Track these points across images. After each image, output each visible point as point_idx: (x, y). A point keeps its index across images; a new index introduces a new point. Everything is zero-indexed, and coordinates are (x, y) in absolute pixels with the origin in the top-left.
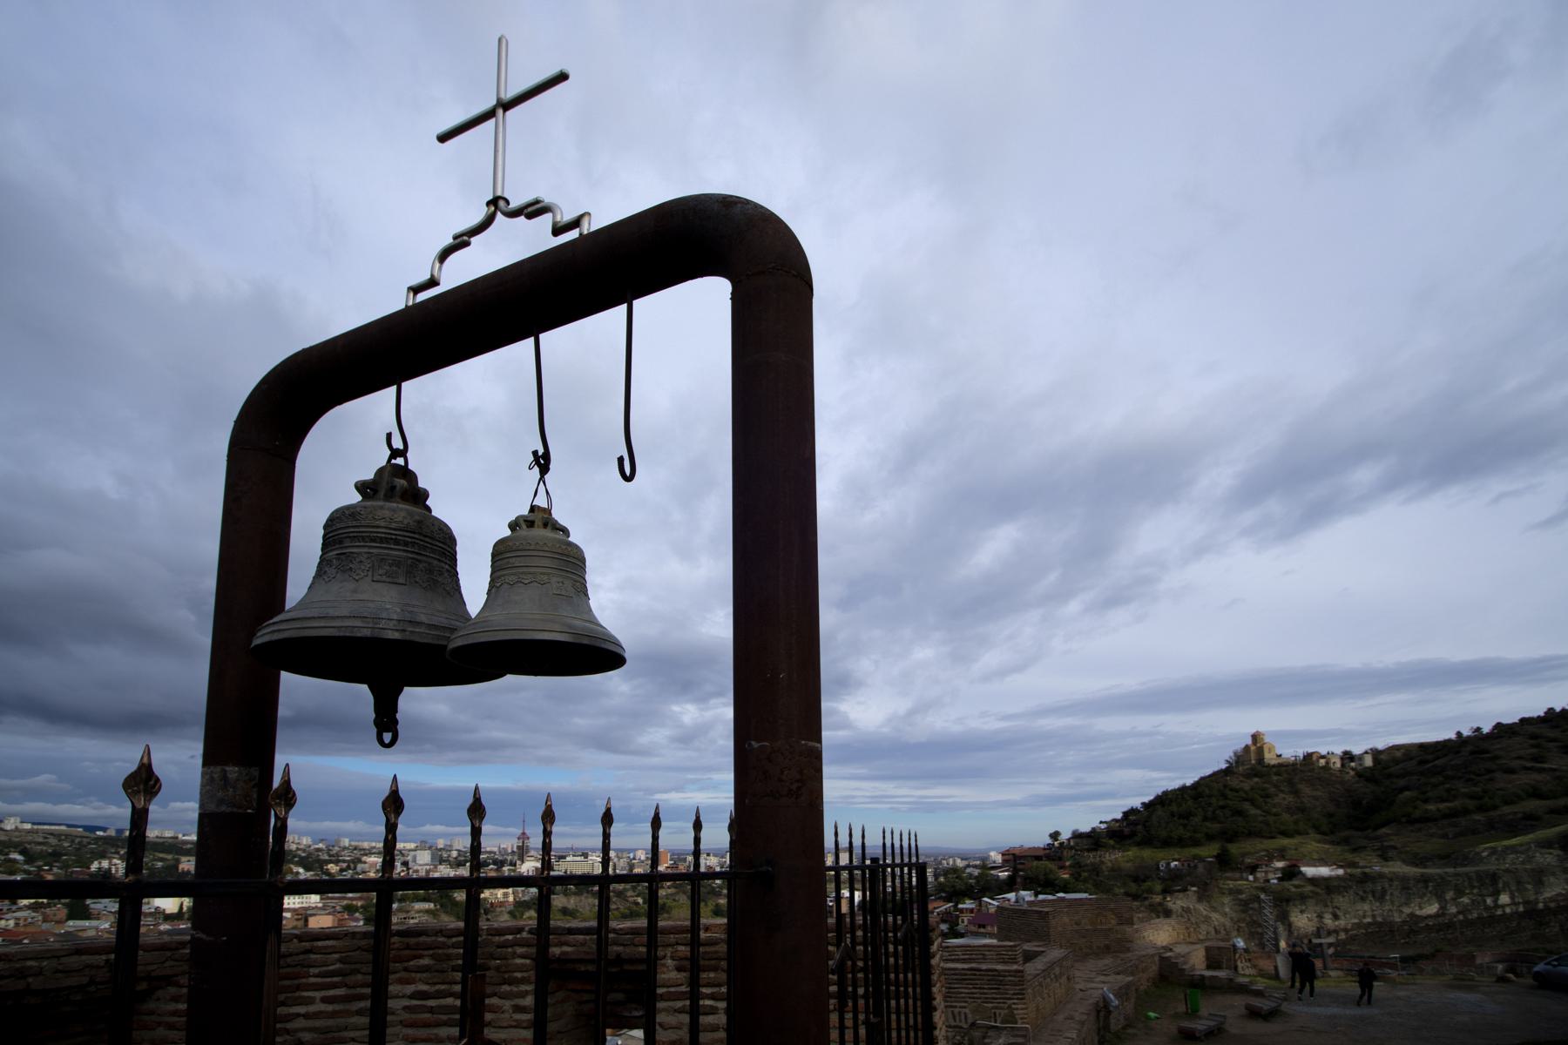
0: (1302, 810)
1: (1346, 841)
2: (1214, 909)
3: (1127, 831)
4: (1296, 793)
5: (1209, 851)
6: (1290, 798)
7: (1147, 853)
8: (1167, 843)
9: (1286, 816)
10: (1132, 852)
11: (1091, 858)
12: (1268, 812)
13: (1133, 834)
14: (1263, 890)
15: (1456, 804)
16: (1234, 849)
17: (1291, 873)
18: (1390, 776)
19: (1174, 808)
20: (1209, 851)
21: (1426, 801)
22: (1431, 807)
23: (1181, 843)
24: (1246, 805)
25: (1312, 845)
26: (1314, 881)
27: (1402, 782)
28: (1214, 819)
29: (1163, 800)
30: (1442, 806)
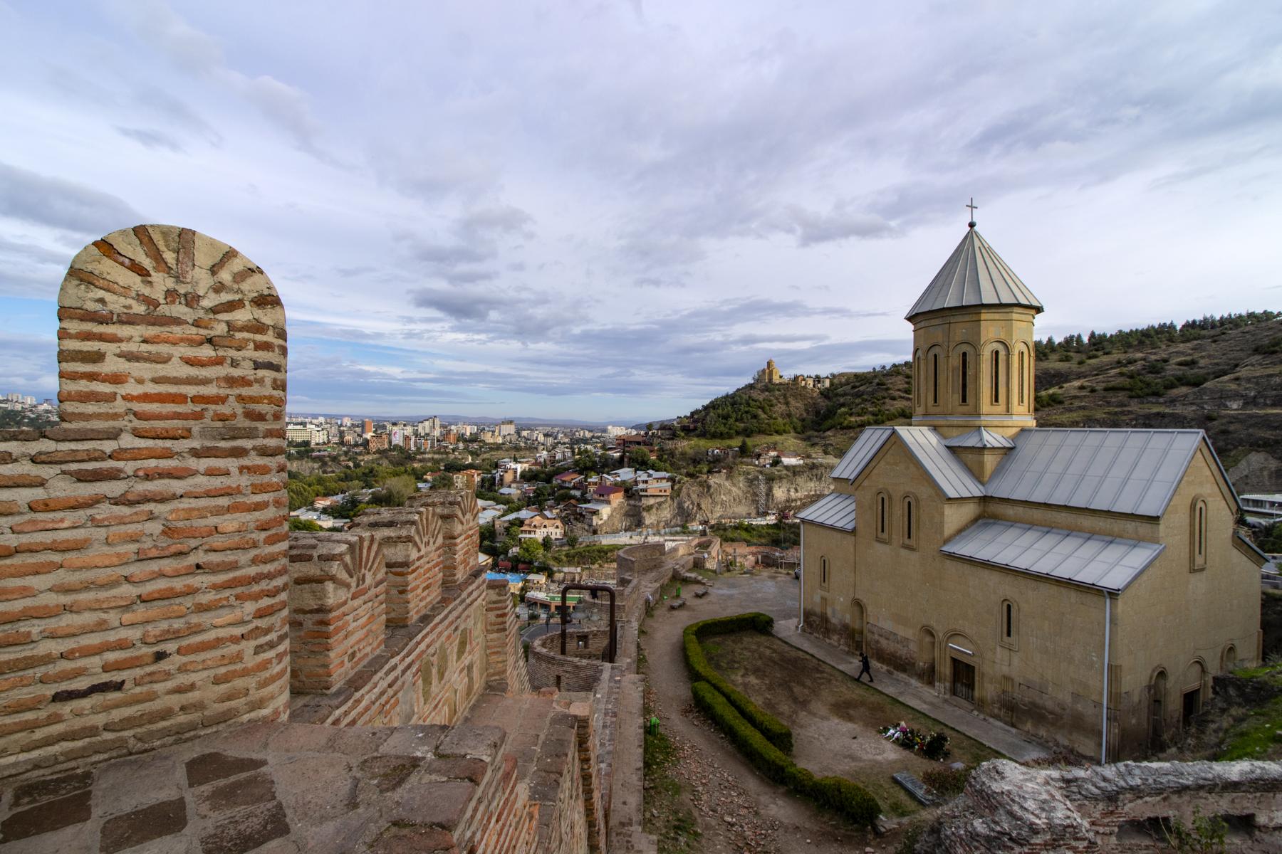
0: (789, 415)
1: (808, 439)
2: (734, 485)
3: (692, 426)
4: (787, 404)
5: (736, 442)
6: (784, 407)
7: (702, 442)
8: (714, 436)
9: (780, 419)
10: (694, 441)
11: (670, 445)
12: (771, 417)
13: (695, 429)
14: (761, 472)
15: (865, 418)
16: (749, 442)
17: (776, 462)
18: (837, 395)
19: (720, 411)
20: (736, 442)
21: (851, 415)
22: (853, 419)
23: (721, 436)
24: (760, 412)
25: (791, 441)
26: (787, 468)
27: (842, 400)
28: (741, 420)
29: (713, 406)
30: (858, 419)
